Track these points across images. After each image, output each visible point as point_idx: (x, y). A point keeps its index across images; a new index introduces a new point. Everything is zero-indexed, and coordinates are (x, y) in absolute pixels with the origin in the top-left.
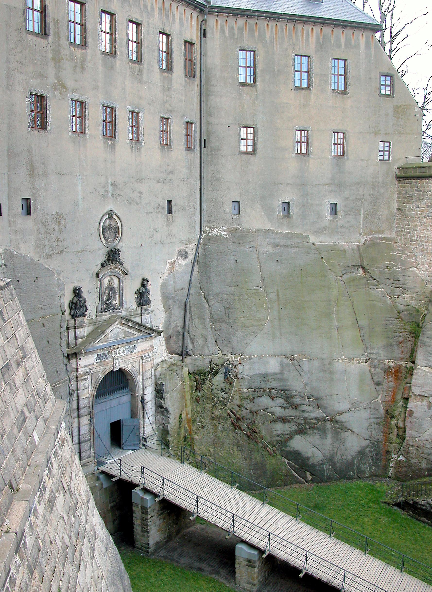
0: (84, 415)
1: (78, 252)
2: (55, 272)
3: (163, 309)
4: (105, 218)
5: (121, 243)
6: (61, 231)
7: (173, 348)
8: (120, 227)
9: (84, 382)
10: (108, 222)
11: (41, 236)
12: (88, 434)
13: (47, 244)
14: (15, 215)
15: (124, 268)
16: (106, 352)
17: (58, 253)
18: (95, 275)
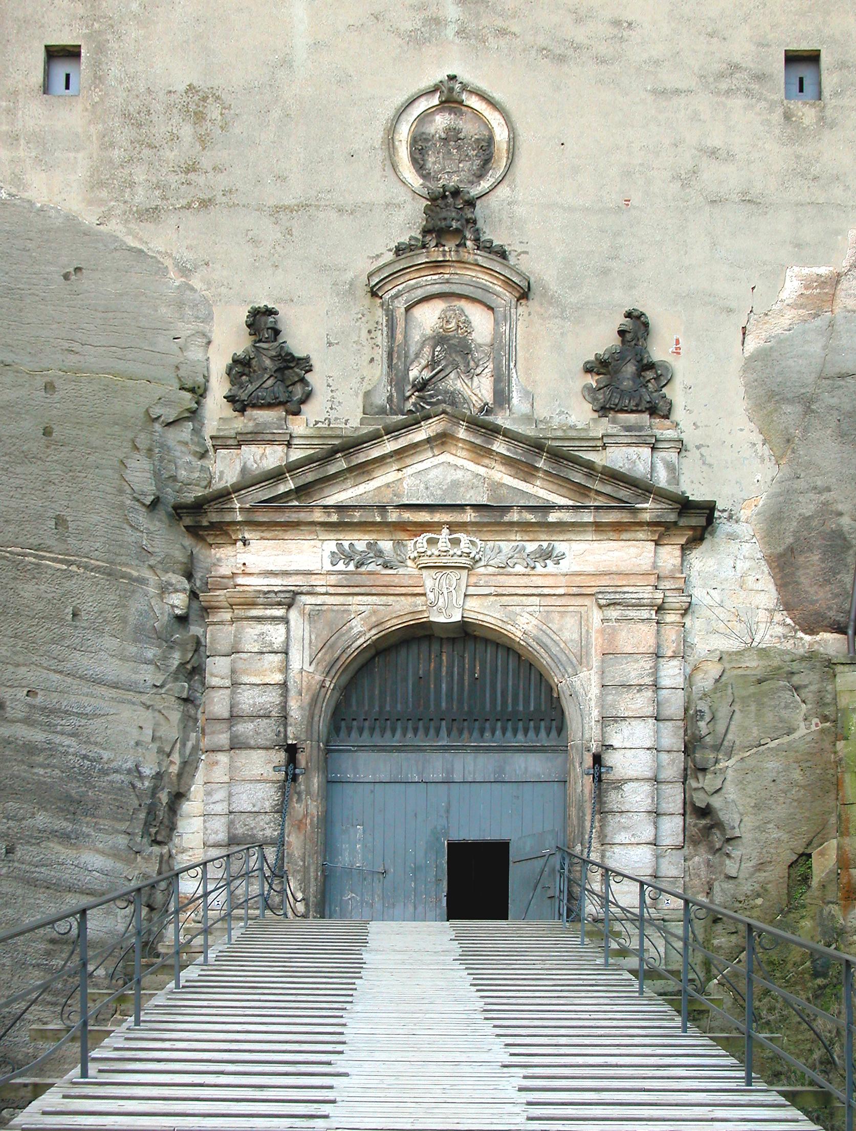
0: (252, 742)
1: (278, 209)
2: (168, 262)
3: (765, 451)
4: (422, 105)
5: (503, 191)
6: (203, 141)
7: (813, 602)
8: (501, 135)
9: (259, 628)
10: (441, 122)
11: (116, 154)
12: (267, 818)
13: (143, 177)
14: (16, 93)
15: (511, 268)
16: (386, 545)
17: (188, 207)
18: (362, 292)
